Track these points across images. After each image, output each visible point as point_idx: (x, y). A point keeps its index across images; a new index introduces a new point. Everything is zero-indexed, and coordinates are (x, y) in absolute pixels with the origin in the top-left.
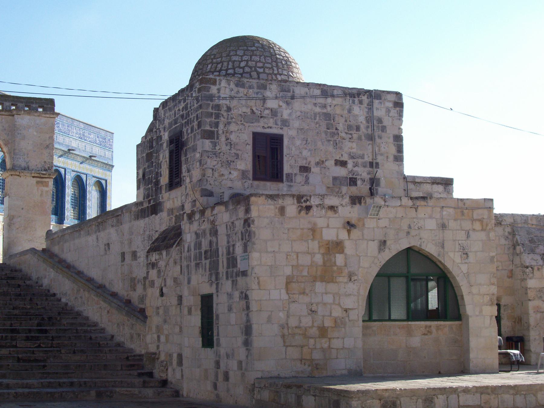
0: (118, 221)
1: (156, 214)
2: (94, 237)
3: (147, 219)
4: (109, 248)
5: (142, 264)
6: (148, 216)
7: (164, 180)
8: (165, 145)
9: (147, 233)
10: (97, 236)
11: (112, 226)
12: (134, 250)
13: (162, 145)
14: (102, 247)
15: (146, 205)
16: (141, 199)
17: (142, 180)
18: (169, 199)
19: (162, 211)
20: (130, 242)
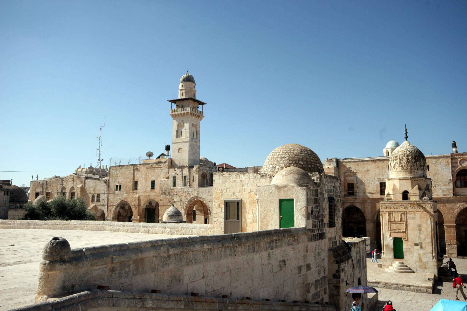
0: (295, 241)
1: (322, 239)
2: (265, 254)
3: (317, 242)
4: (285, 265)
5: (314, 272)
6: (318, 240)
7: (326, 220)
8: (326, 200)
9: (317, 251)
10: (269, 254)
11: (289, 244)
12: (308, 263)
13: (324, 199)
14: (276, 264)
15: (316, 232)
16: (310, 227)
17: (310, 214)
18: (329, 232)
19: (325, 238)
20: (305, 257)
